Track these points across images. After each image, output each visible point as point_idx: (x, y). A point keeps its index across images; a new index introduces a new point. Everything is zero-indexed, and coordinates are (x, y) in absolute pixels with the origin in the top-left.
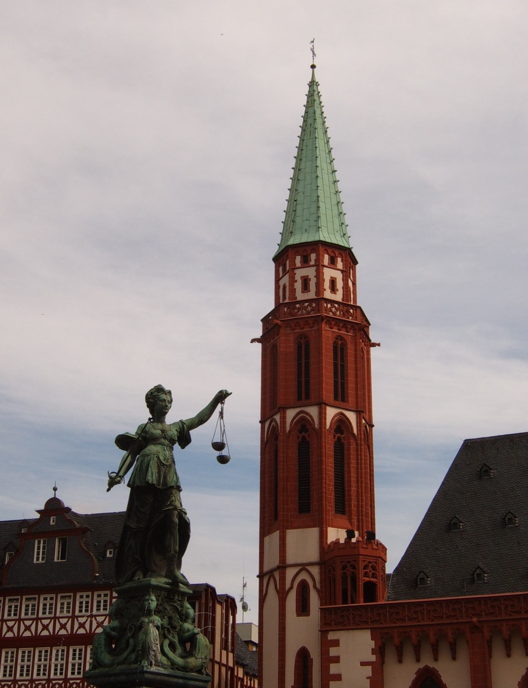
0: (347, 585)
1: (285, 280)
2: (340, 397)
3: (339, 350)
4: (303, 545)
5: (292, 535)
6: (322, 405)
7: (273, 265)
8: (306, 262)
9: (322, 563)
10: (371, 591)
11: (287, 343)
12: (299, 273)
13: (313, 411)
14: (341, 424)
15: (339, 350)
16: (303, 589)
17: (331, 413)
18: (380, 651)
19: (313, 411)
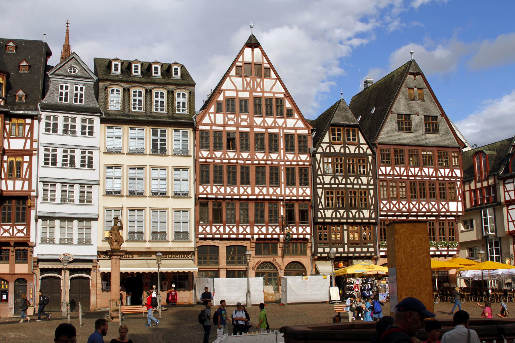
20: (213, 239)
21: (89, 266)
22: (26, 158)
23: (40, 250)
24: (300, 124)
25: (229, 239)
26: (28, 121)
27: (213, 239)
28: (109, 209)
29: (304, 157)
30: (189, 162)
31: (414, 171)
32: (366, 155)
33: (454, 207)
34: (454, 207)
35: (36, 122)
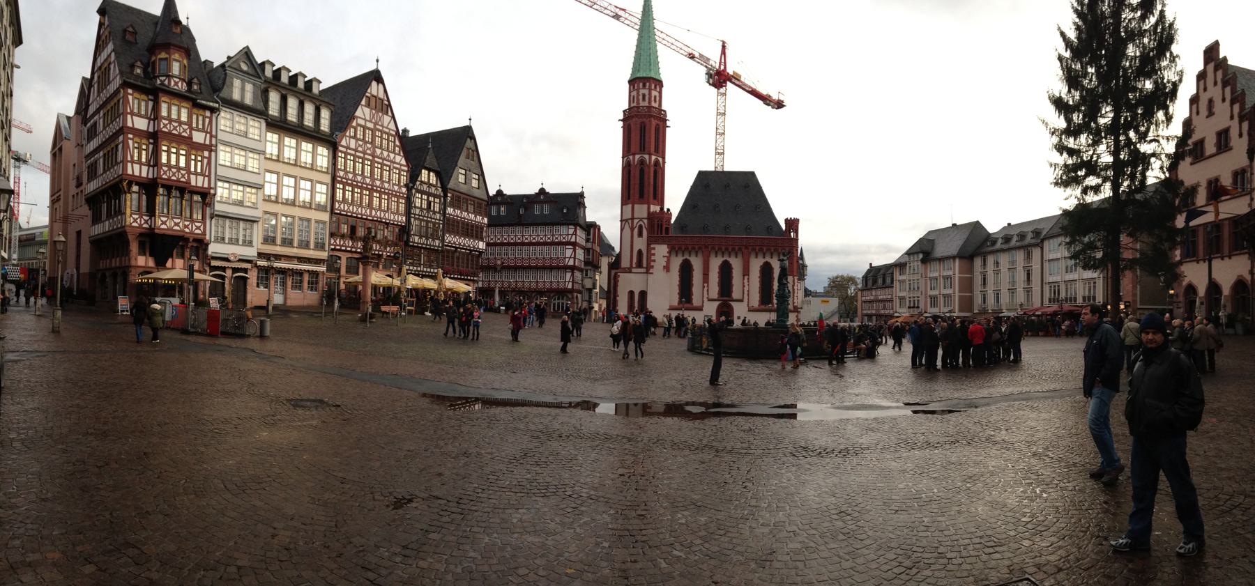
0: (658, 226)
1: (635, 93)
2: (657, 151)
3: (657, 129)
4: (641, 211)
5: (636, 206)
6: (650, 154)
7: (627, 85)
8: (644, 86)
9: (648, 218)
10: (667, 229)
11: (635, 123)
12: (642, 91)
13: (647, 157)
14: (657, 163)
15: (657, 129)
16: (641, 227)
17: (653, 158)
18: (670, 252)
19: (647, 157)
20: (340, 250)
21: (248, 266)
22: (206, 154)
23: (214, 249)
24: (403, 162)
25: (351, 252)
26: (208, 113)
27: (340, 250)
28: (266, 213)
29: (404, 190)
30: (328, 179)
31: (465, 214)
32: (439, 197)
33: (482, 245)
34: (482, 245)
35: (214, 116)
